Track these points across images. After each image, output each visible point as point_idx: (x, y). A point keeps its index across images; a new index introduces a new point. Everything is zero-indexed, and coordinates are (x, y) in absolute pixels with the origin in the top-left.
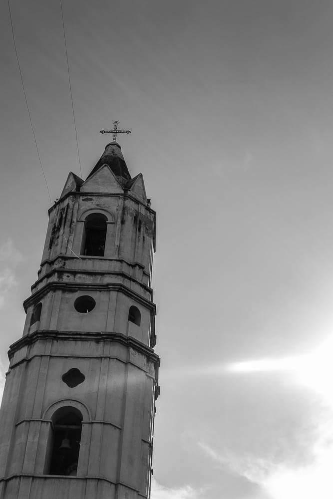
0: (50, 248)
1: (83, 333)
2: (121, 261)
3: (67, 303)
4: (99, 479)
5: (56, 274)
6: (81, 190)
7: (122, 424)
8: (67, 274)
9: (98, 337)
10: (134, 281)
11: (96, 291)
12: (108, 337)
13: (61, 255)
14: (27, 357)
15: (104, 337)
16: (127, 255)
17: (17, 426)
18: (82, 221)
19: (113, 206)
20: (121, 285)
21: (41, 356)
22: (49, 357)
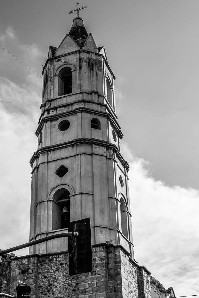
1: (63, 144)
3: (54, 127)
5: (46, 112)
7: (93, 192)
8: (52, 110)
10: (92, 103)
11: (69, 115)
12: (77, 142)
13: (48, 100)
14: (37, 166)
15: (75, 142)
16: (86, 87)
17: (36, 206)
18: (57, 75)
19: (73, 60)
20: (82, 108)
21: (43, 163)
22: (47, 163)
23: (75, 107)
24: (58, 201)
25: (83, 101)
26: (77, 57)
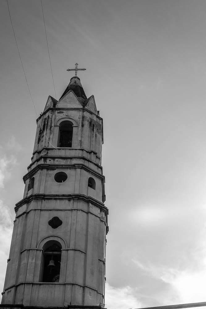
0: (38, 143)
1: (60, 195)
2: (82, 150)
3: (50, 177)
4: (73, 284)
5: (43, 159)
6: (56, 107)
7: (86, 251)
9: (70, 197)
10: (91, 162)
11: (67, 169)
12: (76, 197)
13: (45, 148)
14: (26, 211)
15: (73, 197)
16: (86, 146)
17: (21, 253)
18: (58, 126)
19: (75, 116)
20: (83, 165)
21: (35, 210)
22: (40, 210)
23: (74, 162)
24: (46, 253)
25: (84, 158)
26: (81, 114)
